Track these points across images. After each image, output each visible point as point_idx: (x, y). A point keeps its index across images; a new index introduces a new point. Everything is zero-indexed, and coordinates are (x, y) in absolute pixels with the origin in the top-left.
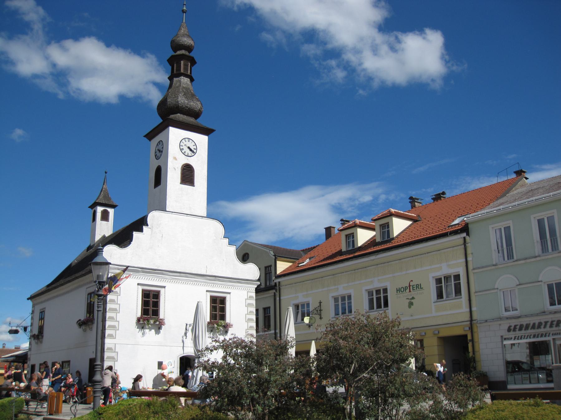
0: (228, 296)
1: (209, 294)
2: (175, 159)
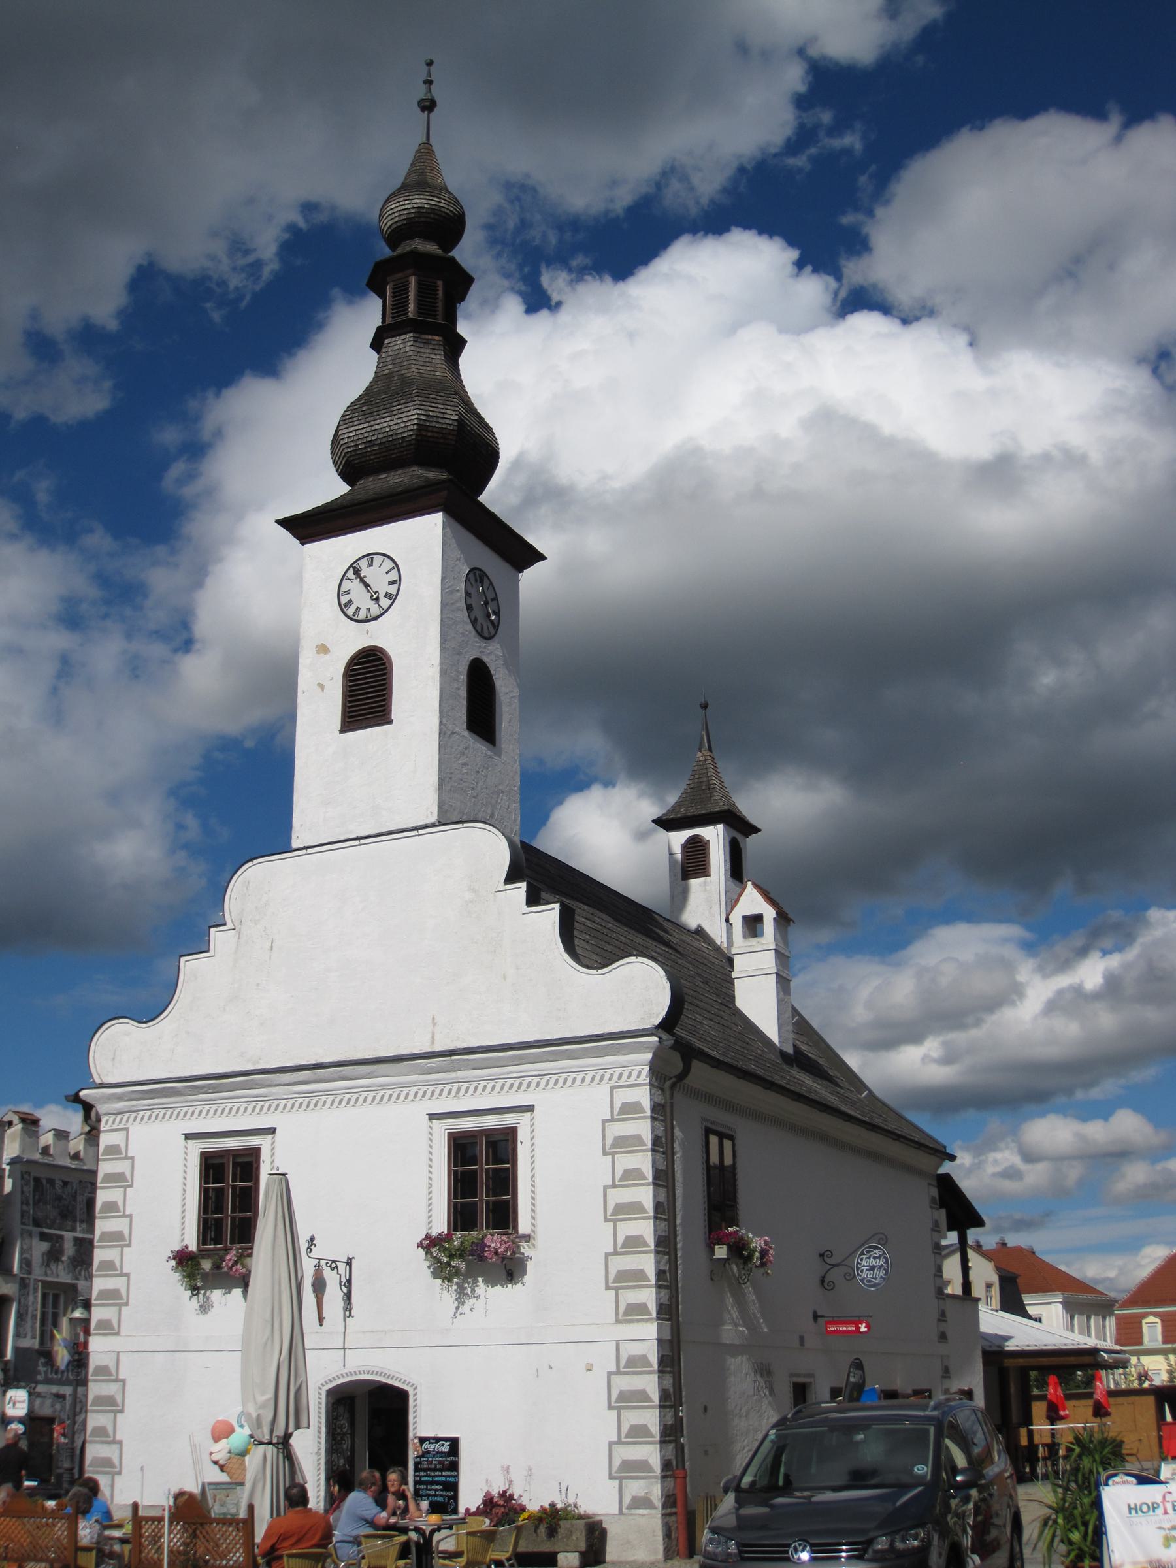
0: (522, 1122)
1: (441, 1131)
2: (323, 649)
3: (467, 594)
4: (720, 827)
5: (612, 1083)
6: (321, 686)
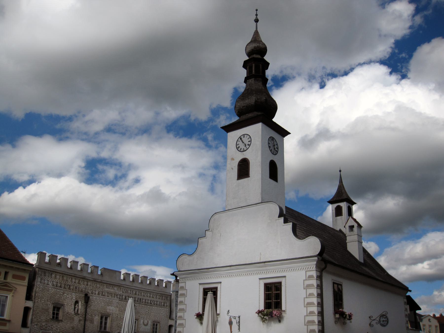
2: (233, 159)
3: (269, 143)
4: (345, 203)
5: (306, 270)
6: (232, 169)
